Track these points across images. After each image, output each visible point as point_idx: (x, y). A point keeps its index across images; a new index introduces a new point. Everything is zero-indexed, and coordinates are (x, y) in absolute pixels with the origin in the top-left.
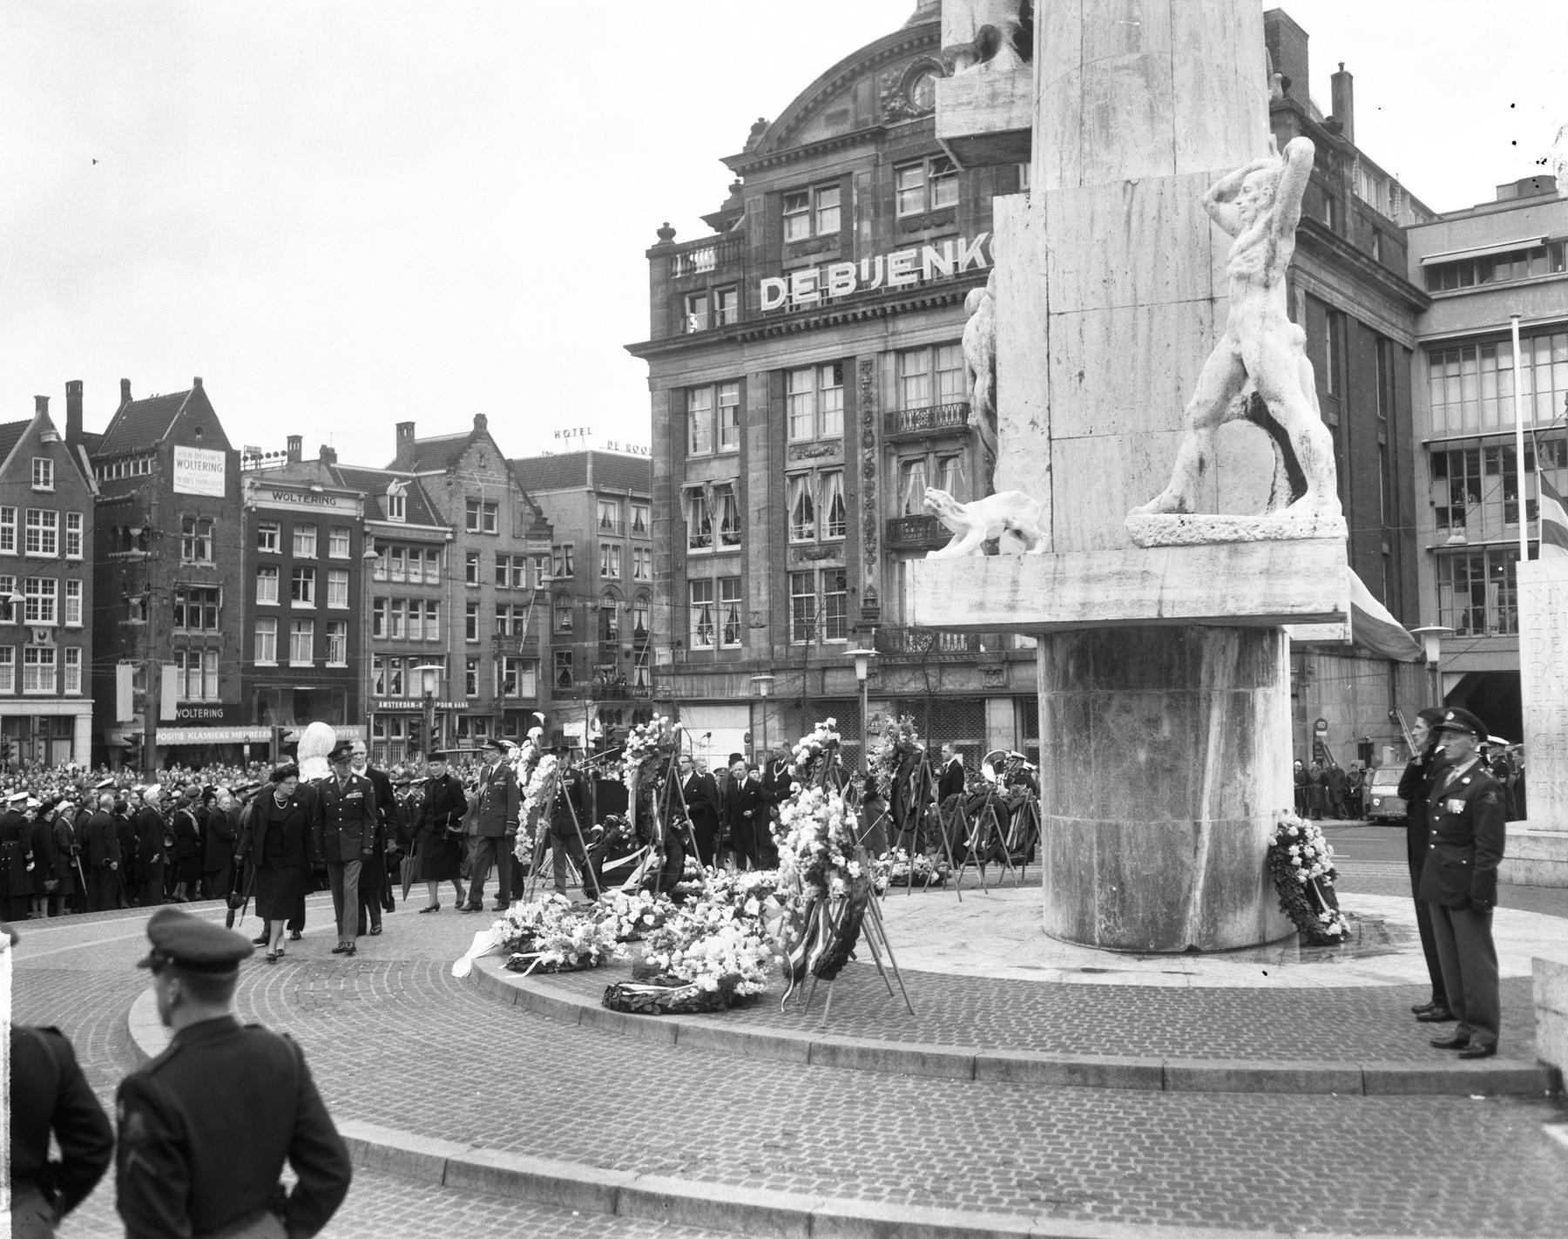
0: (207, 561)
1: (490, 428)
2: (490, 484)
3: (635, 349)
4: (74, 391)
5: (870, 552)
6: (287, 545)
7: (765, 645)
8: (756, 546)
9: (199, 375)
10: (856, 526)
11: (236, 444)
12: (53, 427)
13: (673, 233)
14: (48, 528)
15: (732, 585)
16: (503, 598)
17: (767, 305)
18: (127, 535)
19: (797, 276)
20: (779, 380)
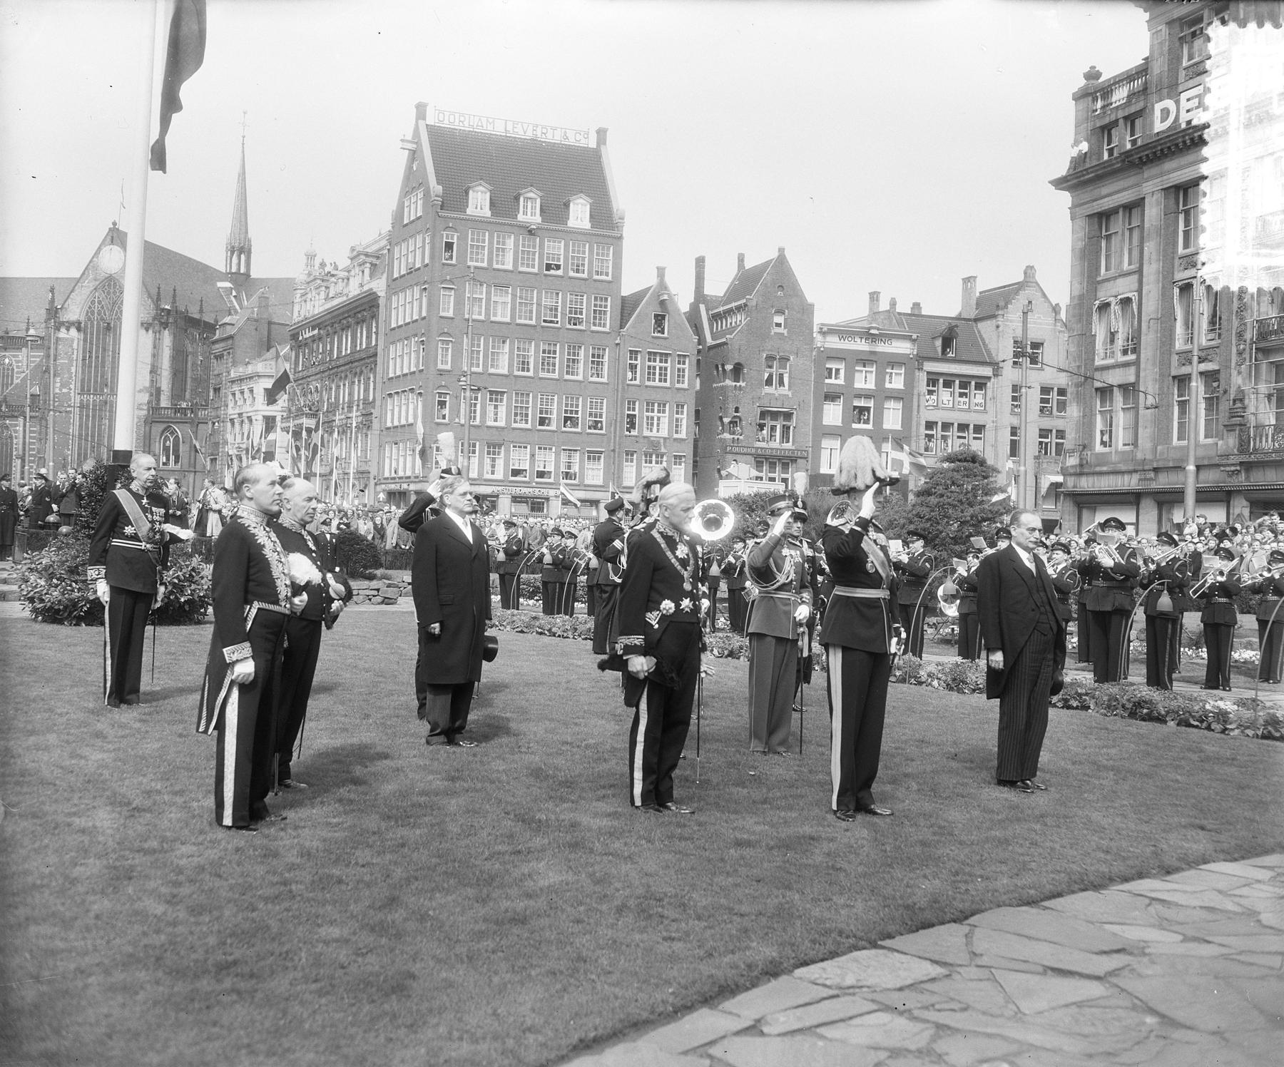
0: (785, 390)
1: (1039, 278)
2: (1041, 326)
3: (1060, 183)
4: (700, 262)
5: (1240, 353)
6: (850, 378)
7: (1149, 445)
8: (1147, 352)
9: (782, 245)
10: (1229, 330)
11: (810, 300)
12: (666, 288)
13: (1098, 75)
14: (663, 365)
15: (1129, 390)
16: (1047, 423)
17: (1159, 126)
18: (724, 370)
19: (1184, 96)
20: (1172, 196)
